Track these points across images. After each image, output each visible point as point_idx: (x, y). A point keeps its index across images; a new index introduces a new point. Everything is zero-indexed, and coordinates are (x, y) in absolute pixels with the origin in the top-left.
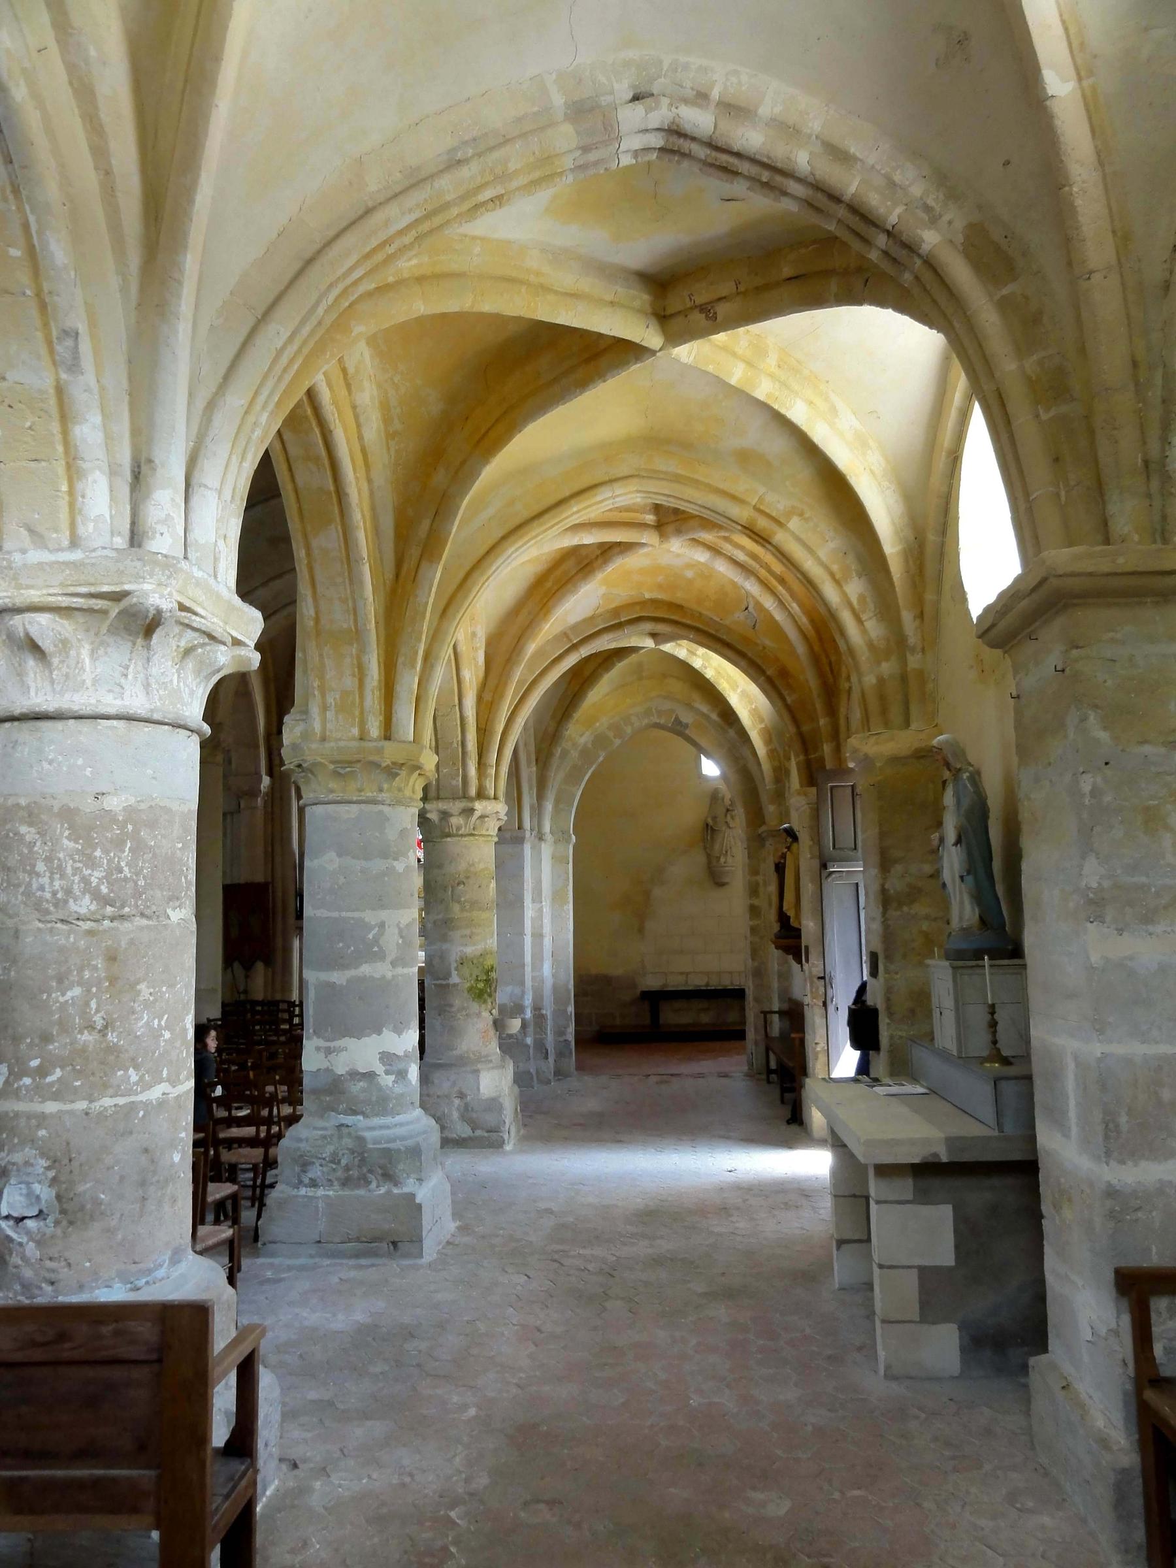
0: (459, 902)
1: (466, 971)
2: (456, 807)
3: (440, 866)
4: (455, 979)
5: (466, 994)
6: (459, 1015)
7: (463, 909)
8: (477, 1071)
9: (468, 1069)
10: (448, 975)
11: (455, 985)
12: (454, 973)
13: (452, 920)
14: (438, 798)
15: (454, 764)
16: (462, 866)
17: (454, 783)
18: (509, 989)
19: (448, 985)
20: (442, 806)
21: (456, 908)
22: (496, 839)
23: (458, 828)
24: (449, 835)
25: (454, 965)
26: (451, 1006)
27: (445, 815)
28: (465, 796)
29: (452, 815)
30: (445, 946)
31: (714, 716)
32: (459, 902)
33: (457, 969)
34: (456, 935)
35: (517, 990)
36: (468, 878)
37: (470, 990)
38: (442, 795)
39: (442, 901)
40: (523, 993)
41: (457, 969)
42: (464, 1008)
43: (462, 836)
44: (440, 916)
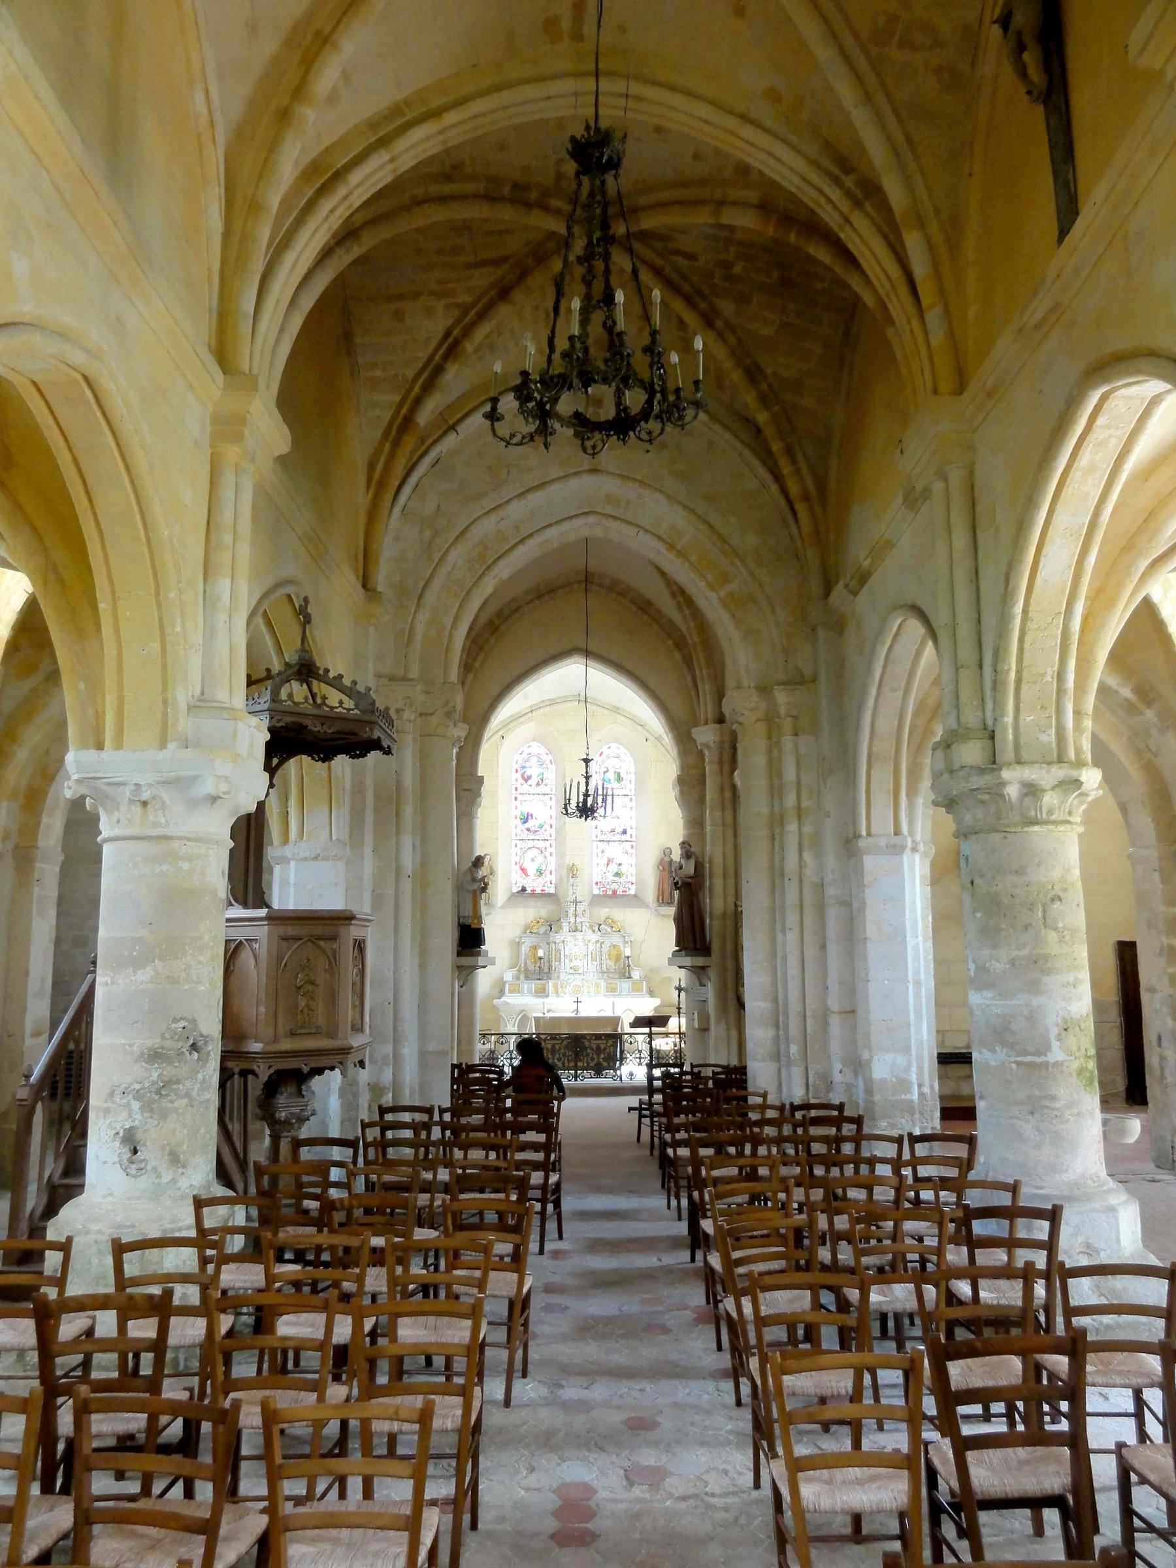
0: (1056, 929)
1: (1072, 1041)
2: (1046, 777)
3: (1020, 872)
4: (1057, 1054)
5: (1074, 1079)
6: (1067, 1113)
7: (1062, 941)
8: (1112, 1209)
9: (1097, 1205)
10: (1048, 1048)
11: (1058, 1064)
12: (1055, 1045)
13: (1047, 958)
14: (1019, 763)
15: (1043, 708)
16: (1056, 874)
17: (1044, 738)
18: (889, 1057)
19: (1046, 1065)
20: (1029, 773)
21: (1053, 936)
22: (1081, 829)
23: (1050, 812)
24: (1035, 822)
25: (1054, 1032)
26: (1054, 1098)
27: (1032, 790)
28: (1060, 760)
29: (1045, 791)
30: (1036, 1001)
31: (1126, 692)
32: (1056, 929)
33: (1059, 1038)
34: (1053, 982)
35: (901, 1060)
36: (1065, 890)
37: (1080, 1071)
38: (1025, 756)
39: (1027, 927)
40: (909, 1065)
41: (1059, 1038)
42: (1071, 1104)
43: (1055, 823)
44: (1025, 952)
